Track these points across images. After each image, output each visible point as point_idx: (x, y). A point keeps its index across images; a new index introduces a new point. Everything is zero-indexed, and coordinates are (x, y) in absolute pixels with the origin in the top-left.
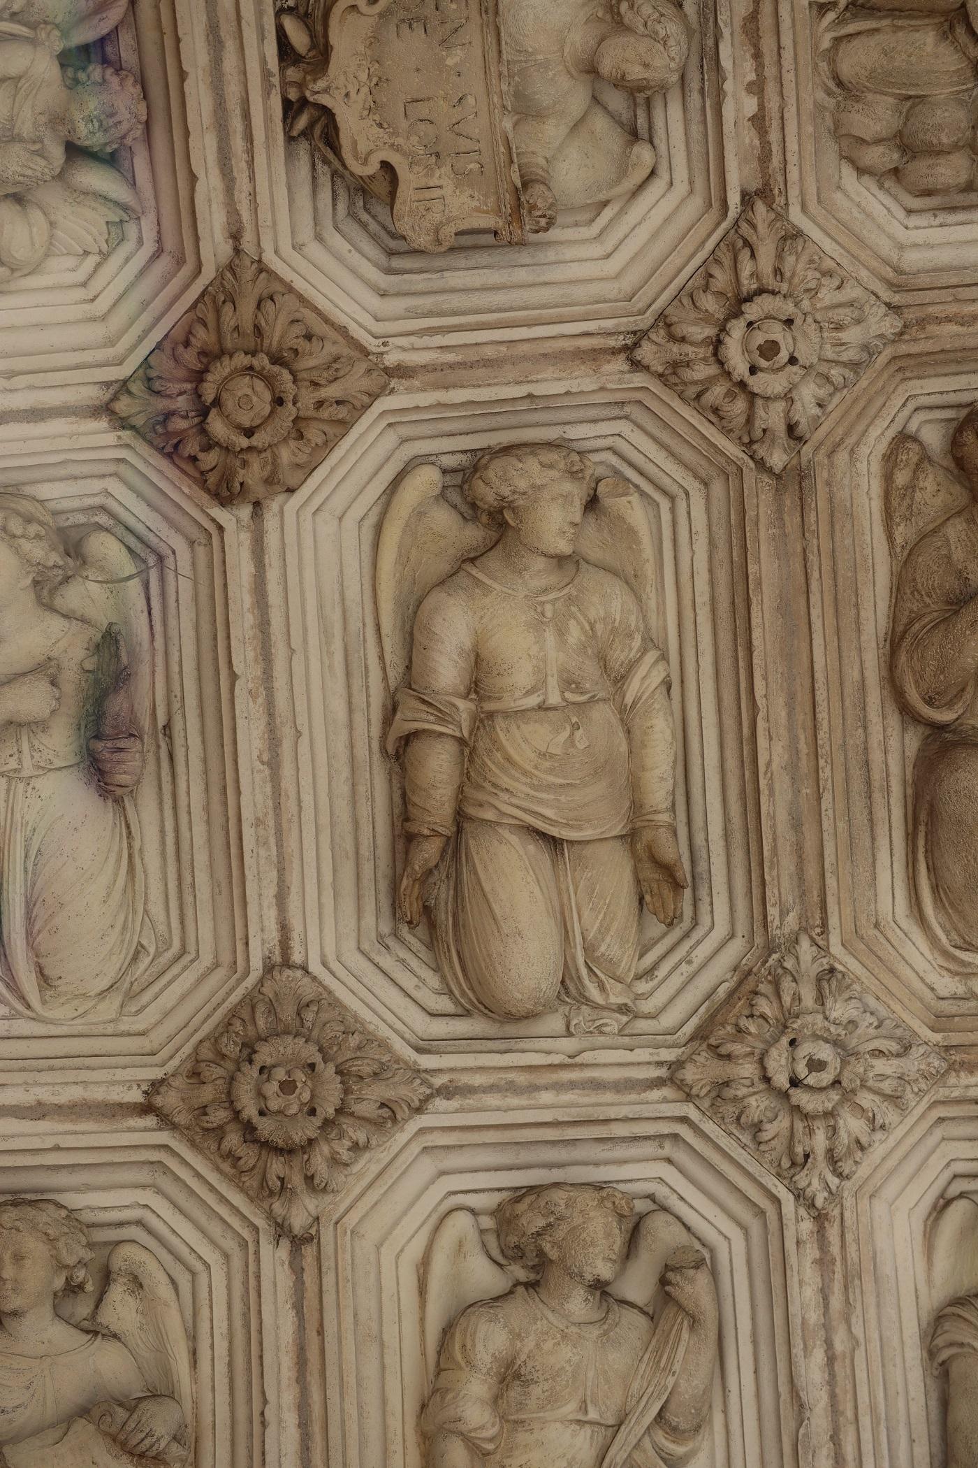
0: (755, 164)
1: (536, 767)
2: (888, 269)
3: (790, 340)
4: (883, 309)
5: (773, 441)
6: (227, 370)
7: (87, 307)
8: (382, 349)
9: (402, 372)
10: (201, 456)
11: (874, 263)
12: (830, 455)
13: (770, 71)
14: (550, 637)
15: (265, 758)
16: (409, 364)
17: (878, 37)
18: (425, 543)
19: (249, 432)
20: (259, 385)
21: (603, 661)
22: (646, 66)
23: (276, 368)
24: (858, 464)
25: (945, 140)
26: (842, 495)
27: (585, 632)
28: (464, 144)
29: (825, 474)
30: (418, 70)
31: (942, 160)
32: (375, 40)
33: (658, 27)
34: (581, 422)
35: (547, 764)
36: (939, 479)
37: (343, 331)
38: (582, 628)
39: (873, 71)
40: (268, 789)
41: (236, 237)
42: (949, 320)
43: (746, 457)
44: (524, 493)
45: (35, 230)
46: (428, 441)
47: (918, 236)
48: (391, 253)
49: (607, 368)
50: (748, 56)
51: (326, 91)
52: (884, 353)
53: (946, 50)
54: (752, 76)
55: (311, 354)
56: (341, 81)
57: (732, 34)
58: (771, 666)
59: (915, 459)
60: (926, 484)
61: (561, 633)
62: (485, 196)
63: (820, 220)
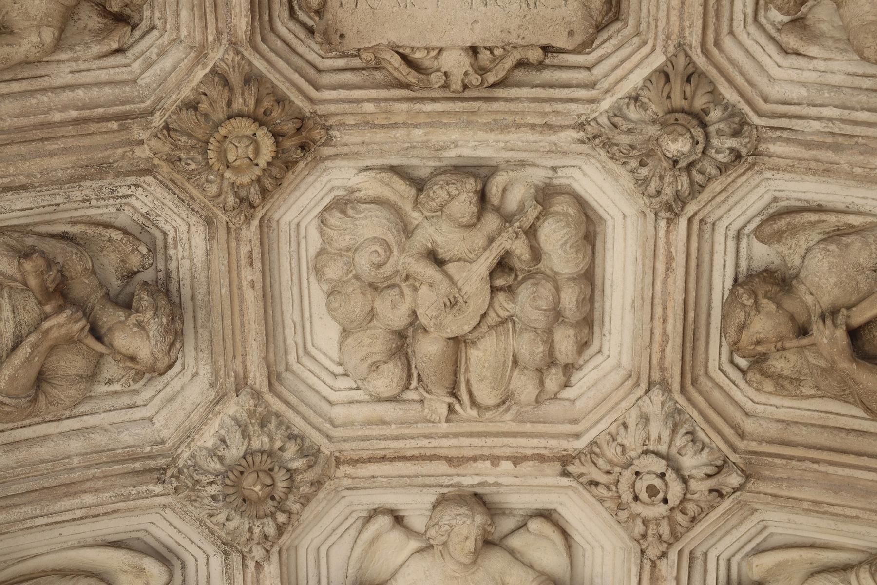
0: (545, 465)
2: (626, 383)
4: (646, 398)
11: (622, 392)
12: (742, 436)
13: (486, 452)
17: (473, 381)
22: (467, 538)
24: (758, 411)
25: (541, 349)
26: (773, 431)
29: (754, 443)
31: (557, 346)
33: (443, 529)
34: (705, 580)
36: (778, 357)
39: (493, 388)
42: (663, 351)
43: (733, 496)
47: (614, 353)
49: (664, 572)
50: (474, 465)
52: (678, 400)
53: (482, 344)
54: (488, 463)
57: (458, 475)
59: (758, 376)
60: (779, 366)
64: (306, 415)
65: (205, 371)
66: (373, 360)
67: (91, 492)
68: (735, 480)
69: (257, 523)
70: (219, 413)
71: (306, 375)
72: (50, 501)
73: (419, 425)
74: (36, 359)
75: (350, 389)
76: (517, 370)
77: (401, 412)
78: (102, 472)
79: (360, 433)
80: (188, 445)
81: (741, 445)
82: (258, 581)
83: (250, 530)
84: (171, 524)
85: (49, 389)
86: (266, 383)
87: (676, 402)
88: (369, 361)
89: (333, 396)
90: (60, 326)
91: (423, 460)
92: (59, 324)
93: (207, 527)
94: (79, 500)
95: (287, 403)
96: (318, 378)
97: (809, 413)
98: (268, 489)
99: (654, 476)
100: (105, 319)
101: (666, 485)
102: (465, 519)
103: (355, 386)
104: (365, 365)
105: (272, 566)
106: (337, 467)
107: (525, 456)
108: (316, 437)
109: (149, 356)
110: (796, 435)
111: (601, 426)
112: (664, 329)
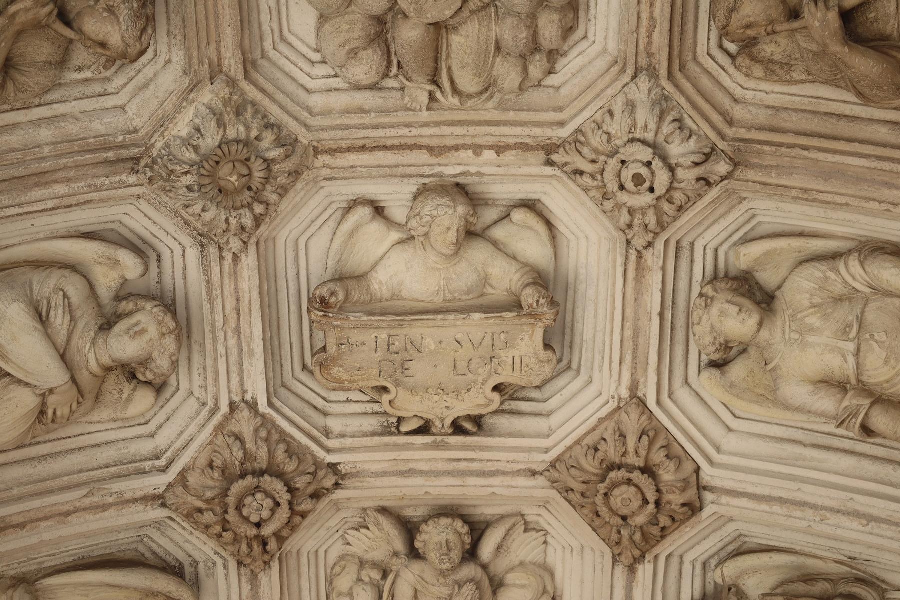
0: (529, 154)
1: (894, 368)
3: (634, 165)
4: (632, 85)
5: (709, 172)
6: (604, 509)
7: (575, 553)
8: (616, 399)
9: (634, 387)
10: (662, 525)
11: (607, 79)
12: (731, 123)
13: (468, 141)
14: (812, 339)
15: (865, 522)
16: (629, 383)
17: (455, 68)
18: (754, 382)
19: (646, 502)
20: (616, 492)
21: (838, 300)
22: (449, 229)
23: (608, 481)
25: (524, 35)
26: (762, 117)
27: (816, 313)
28: (488, 341)
29: (743, 130)
30: (436, 366)
31: (541, 32)
32: (413, 391)
33: (425, 220)
34: (692, 270)
35: (893, 362)
36: (768, 41)
37: (601, 421)
38: (812, 314)
40: (884, 526)
41: (534, 473)
42: (650, 36)
44: (715, 338)
45: (518, 582)
46: (690, 367)
47: (600, 38)
48: (569, 367)
49: (650, 263)
50: (457, 154)
51: (442, 420)
52: (665, 86)
53: (464, 30)
55: (606, 451)
56: (438, 412)
57: (440, 165)
58: (863, 194)
59: (748, 61)
60: (769, 51)
61: (812, 330)
62: (522, 332)
63: (573, 112)
64: (284, 104)
65: (178, 58)
66: (352, 47)
67: (62, 182)
68: (723, 168)
69: (234, 214)
70: (194, 102)
71: (283, 62)
72: (21, 191)
73: (399, 114)
74: (3, 44)
75: (329, 77)
76: (500, 56)
77: (381, 101)
78: (74, 162)
79: (339, 122)
80: (162, 135)
81: (730, 132)
82: (235, 273)
83: (227, 221)
84: (145, 215)
85: (17, 76)
86: (241, 70)
87: (664, 89)
88: (347, 48)
89: (311, 84)
90: (27, 10)
91: (404, 149)
92: (26, 7)
93: (183, 218)
94: (51, 190)
95: (263, 91)
96: (296, 65)
97: (799, 99)
98: (244, 180)
99: (641, 165)
100: (74, 4)
101: (653, 173)
102: (447, 210)
103: (333, 73)
104: (344, 52)
105: (250, 258)
106: (316, 157)
107: (508, 145)
108: (293, 126)
109: (120, 42)
110: (786, 121)
111: (587, 114)
112: (652, 13)
